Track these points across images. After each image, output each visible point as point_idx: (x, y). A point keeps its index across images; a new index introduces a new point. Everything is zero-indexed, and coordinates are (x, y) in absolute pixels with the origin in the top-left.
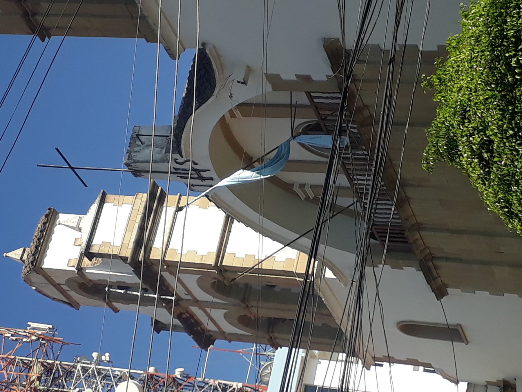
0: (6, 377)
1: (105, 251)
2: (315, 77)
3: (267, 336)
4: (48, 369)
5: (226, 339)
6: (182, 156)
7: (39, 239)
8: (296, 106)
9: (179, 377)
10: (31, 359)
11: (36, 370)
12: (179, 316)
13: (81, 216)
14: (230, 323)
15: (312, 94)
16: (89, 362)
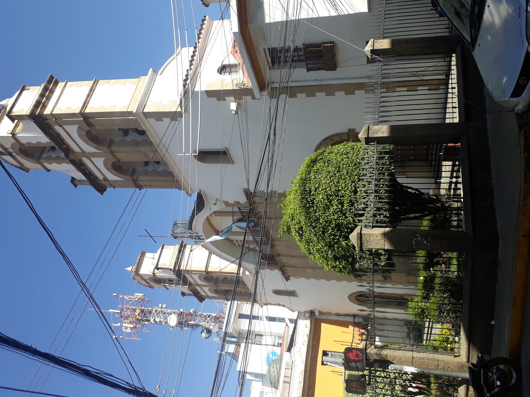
0: (126, 314)
1: (163, 267)
2: (240, 202)
3: (224, 297)
4: (142, 311)
5: (209, 298)
6: (192, 231)
7: (138, 263)
8: (235, 212)
9: (192, 312)
10: (136, 307)
11: (138, 311)
12: (191, 291)
13: (155, 254)
14: (211, 293)
15: (240, 208)
16: (158, 308)
